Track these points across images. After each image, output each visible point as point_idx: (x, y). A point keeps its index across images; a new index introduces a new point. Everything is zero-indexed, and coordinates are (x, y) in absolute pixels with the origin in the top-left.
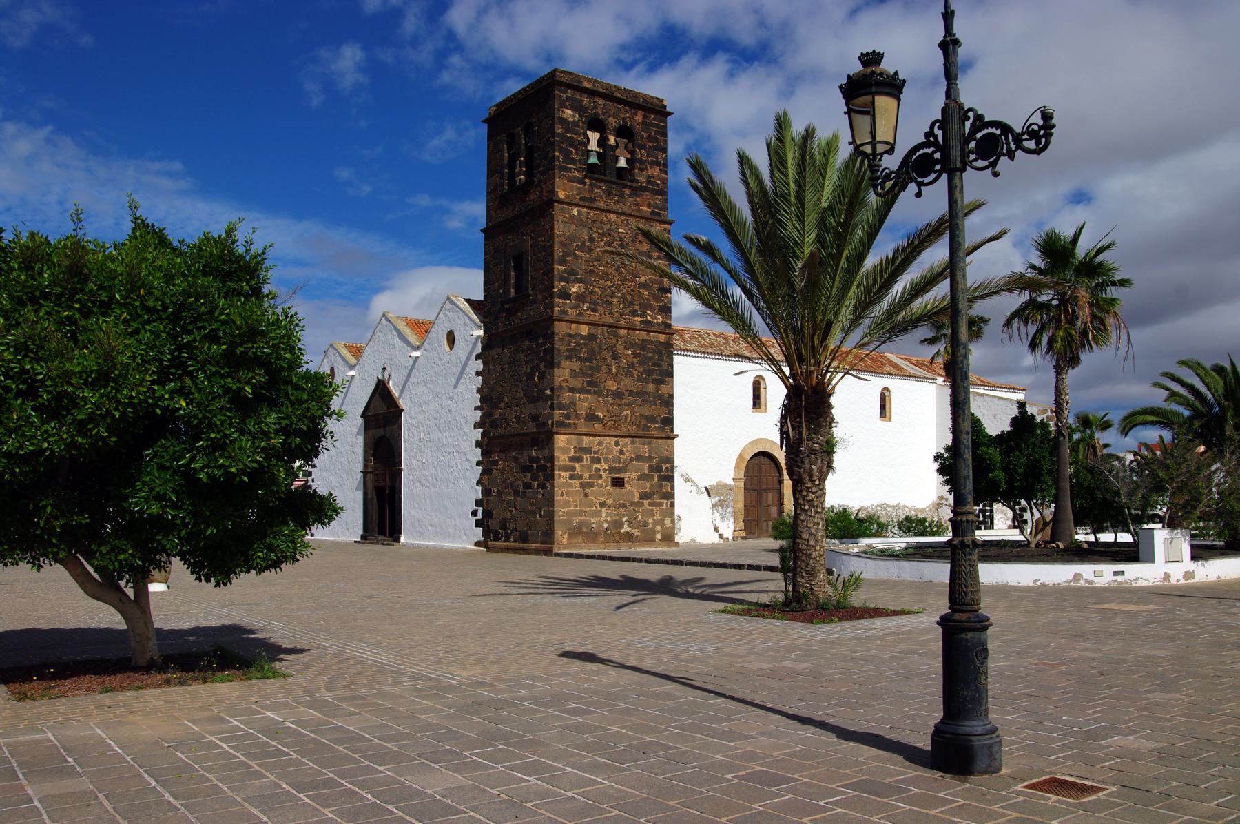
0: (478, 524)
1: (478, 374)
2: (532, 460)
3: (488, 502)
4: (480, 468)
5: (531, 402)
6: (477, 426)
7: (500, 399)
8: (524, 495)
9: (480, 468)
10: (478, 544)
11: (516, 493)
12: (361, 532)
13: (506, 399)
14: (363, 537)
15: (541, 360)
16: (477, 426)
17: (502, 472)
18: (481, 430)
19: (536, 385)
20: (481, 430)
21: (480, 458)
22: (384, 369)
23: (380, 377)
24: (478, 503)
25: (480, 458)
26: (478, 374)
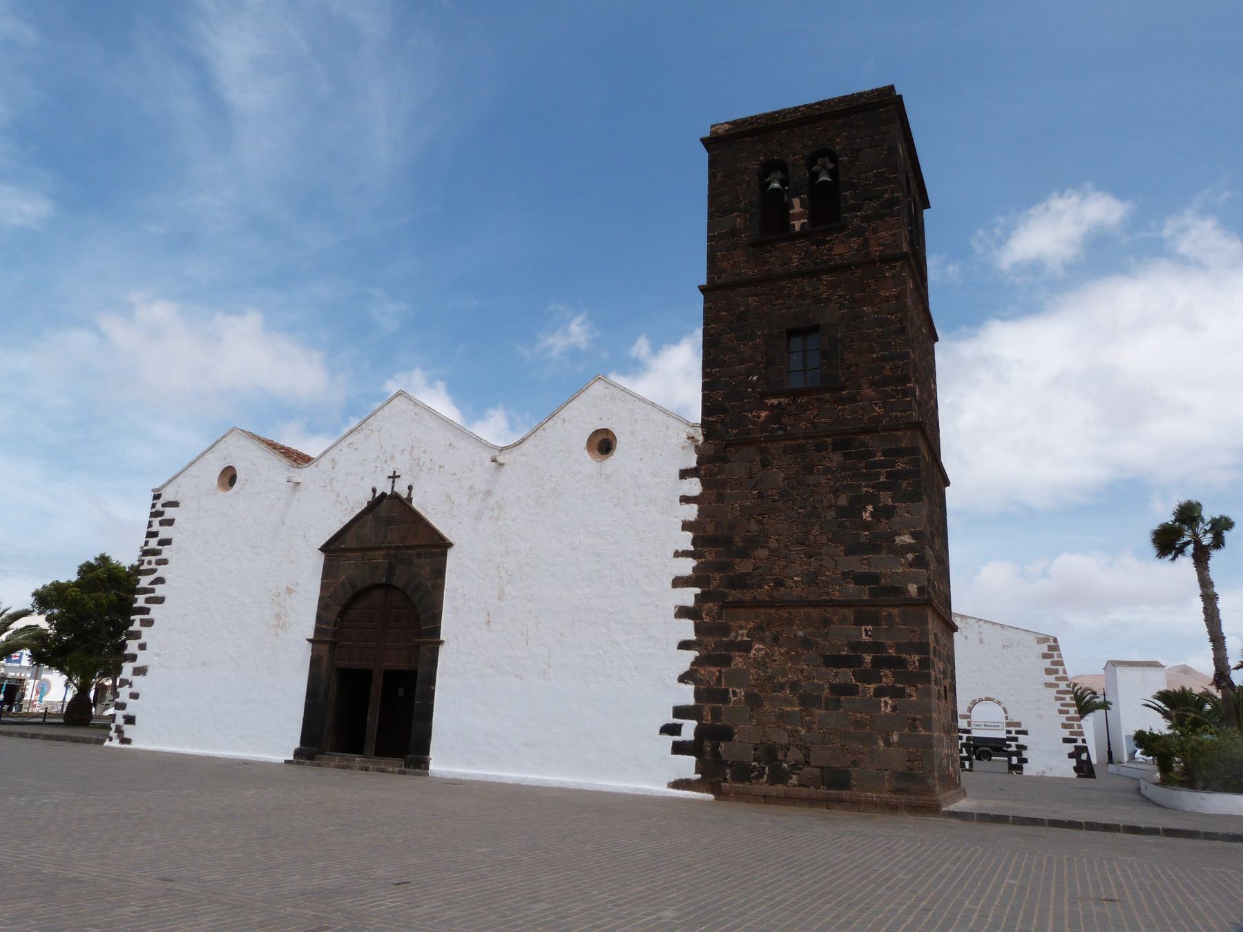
0: (678, 748)
1: (685, 499)
2: (859, 647)
3: (716, 714)
4: (691, 655)
5: (850, 551)
6: (679, 582)
7: (754, 542)
8: (833, 705)
9: (691, 655)
10: (678, 784)
11: (808, 701)
12: (296, 743)
13: (773, 544)
14: (297, 753)
15: (880, 487)
16: (679, 582)
17: (760, 664)
18: (698, 590)
19: (866, 526)
20: (698, 590)
21: (692, 636)
22: (394, 477)
23: (384, 487)
24: (680, 712)
25: (692, 636)
26: (685, 499)
